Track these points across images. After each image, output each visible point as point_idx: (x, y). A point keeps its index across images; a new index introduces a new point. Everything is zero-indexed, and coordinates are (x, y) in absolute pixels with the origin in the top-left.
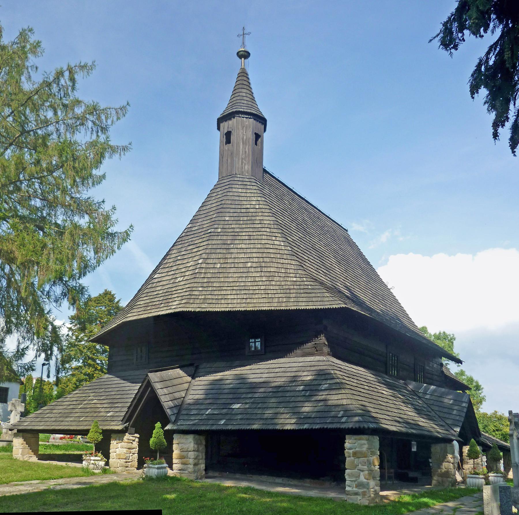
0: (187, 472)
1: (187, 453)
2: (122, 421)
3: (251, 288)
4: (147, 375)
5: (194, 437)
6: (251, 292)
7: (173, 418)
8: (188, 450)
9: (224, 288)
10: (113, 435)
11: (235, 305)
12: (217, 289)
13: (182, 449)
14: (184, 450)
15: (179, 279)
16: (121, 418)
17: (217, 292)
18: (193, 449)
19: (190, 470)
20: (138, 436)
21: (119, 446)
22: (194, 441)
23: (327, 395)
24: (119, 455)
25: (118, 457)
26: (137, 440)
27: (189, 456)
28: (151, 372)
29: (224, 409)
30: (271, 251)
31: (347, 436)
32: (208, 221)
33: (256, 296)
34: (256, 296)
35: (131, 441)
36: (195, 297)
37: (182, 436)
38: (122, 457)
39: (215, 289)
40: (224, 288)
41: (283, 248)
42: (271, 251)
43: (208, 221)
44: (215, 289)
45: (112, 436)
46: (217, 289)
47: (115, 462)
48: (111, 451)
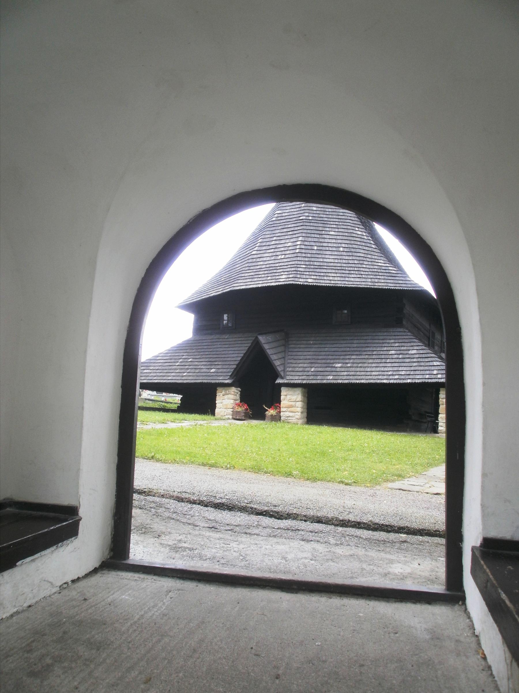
0: (294, 418)
1: (295, 403)
2: (230, 376)
3: (346, 269)
4: (257, 337)
5: (302, 390)
6: (347, 272)
7: (282, 374)
8: (297, 400)
9: (324, 267)
10: (219, 389)
11: (337, 282)
12: (318, 267)
13: (290, 399)
14: (292, 400)
15: (280, 257)
16: (230, 374)
17: (319, 269)
18: (301, 400)
19: (298, 417)
20: (239, 389)
22: (302, 394)
23: (418, 358)
24: (226, 405)
25: (225, 407)
26: (239, 393)
27: (297, 406)
28: (261, 334)
29: (327, 367)
30: (357, 239)
31: (441, 389)
32: (297, 210)
33: (353, 276)
34: (353, 276)
35: (236, 394)
36: (300, 273)
37: (290, 389)
39: (316, 267)
40: (324, 267)
41: (365, 237)
42: (357, 239)
43: (297, 210)
44: (316, 267)
45: (217, 389)
46: (318, 267)
47: (221, 411)
48: (217, 402)
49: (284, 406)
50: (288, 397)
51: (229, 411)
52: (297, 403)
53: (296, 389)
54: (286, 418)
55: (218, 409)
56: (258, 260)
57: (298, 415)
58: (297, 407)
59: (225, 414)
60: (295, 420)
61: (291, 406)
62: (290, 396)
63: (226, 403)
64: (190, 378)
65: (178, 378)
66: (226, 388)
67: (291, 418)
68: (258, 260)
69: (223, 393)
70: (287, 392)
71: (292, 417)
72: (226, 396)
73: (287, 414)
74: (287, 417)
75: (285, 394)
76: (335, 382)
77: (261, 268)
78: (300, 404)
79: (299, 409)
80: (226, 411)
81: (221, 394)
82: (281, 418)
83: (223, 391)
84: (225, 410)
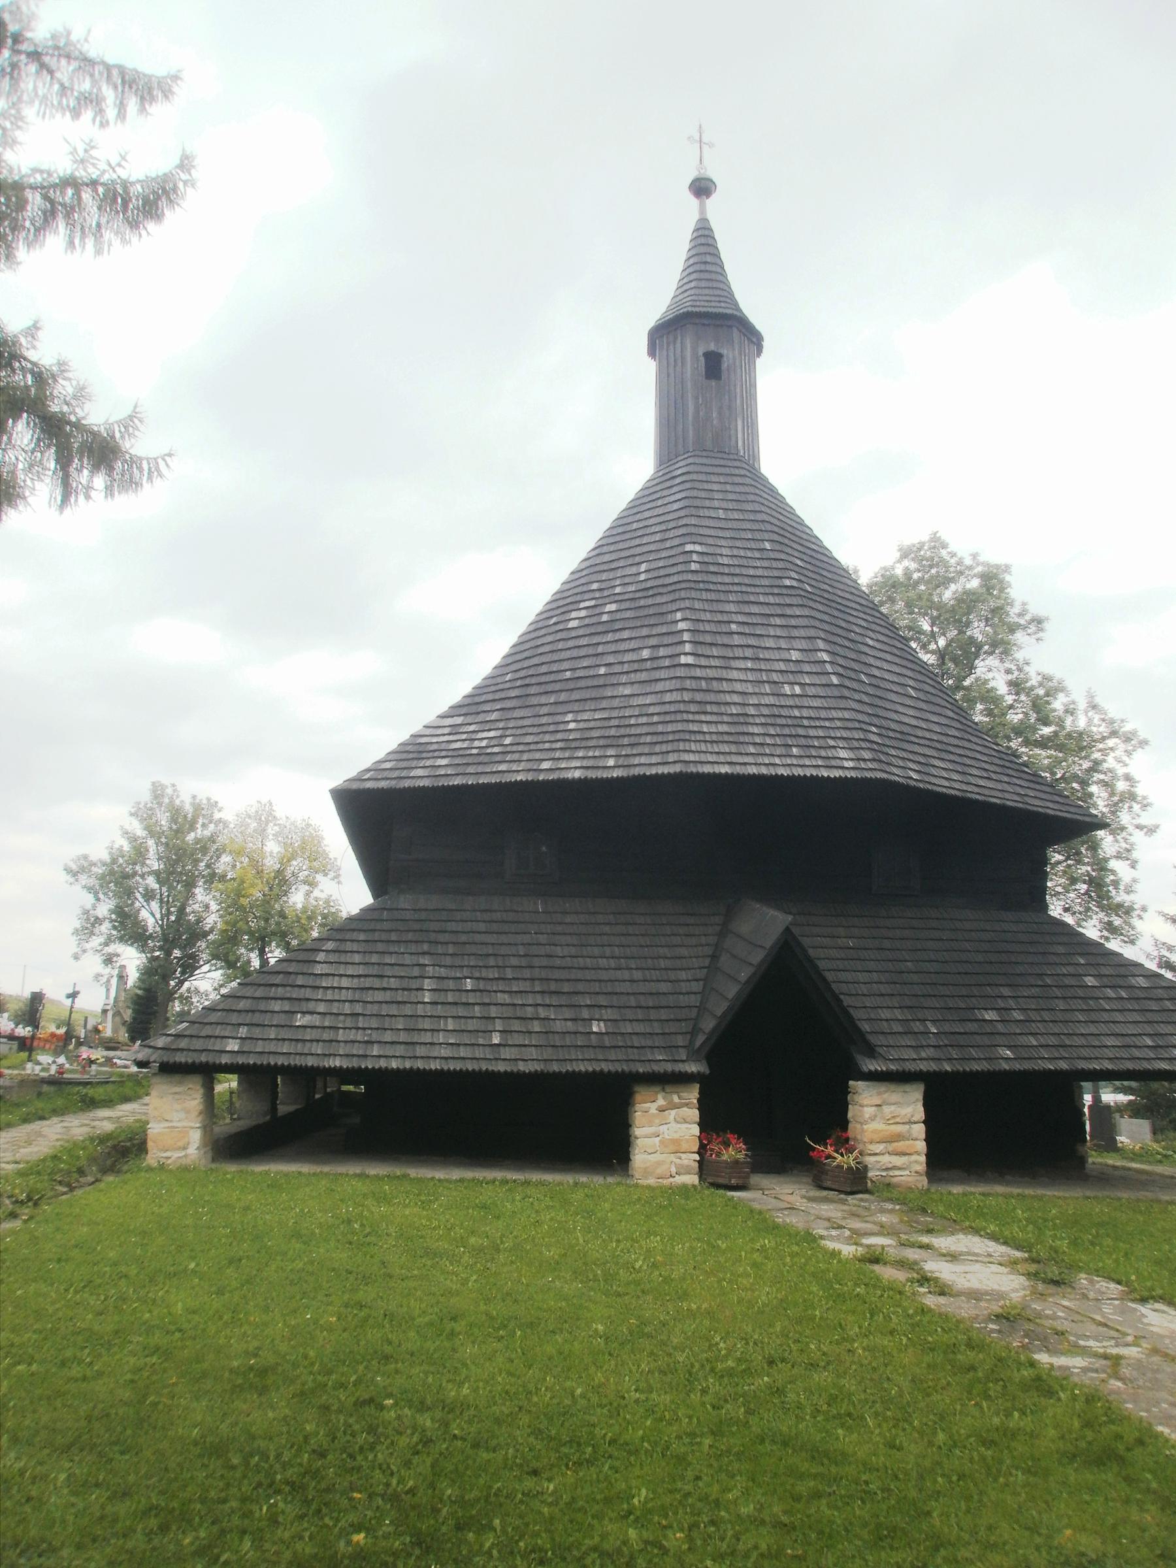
0: (907, 1172)
1: (907, 1127)
8: (915, 1119)
14: (898, 1120)
21: (672, 1117)
25: (672, 1148)
37: (893, 1087)
38: (685, 1147)
47: (659, 1163)
49: (876, 1137)
50: (887, 1110)
51: (686, 1162)
52: (914, 1126)
53: (907, 1087)
54: (884, 1174)
55: (646, 1156)
56: (715, 685)
57: (920, 1161)
58: (916, 1139)
59: (674, 1170)
60: (910, 1179)
61: (899, 1137)
62: (893, 1108)
63: (676, 1136)
64: (533, 1053)
65: (479, 1053)
66: (668, 1088)
67: (897, 1173)
68: (715, 685)
69: (661, 1101)
70: (885, 1096)
71: (899, 1169)
72: (673, 1112)
73: (886, 1160)
74: (887, 1169)
75: (879, 1102)
76: (1017, 1066)
77: (780, 716)
78: (920, 1130)
79: (922, 1146)
80: (678, 1161)
81: (653, 1108)
82: (870, 1174)
83: (660, 1096)
84: (672, 1157)
